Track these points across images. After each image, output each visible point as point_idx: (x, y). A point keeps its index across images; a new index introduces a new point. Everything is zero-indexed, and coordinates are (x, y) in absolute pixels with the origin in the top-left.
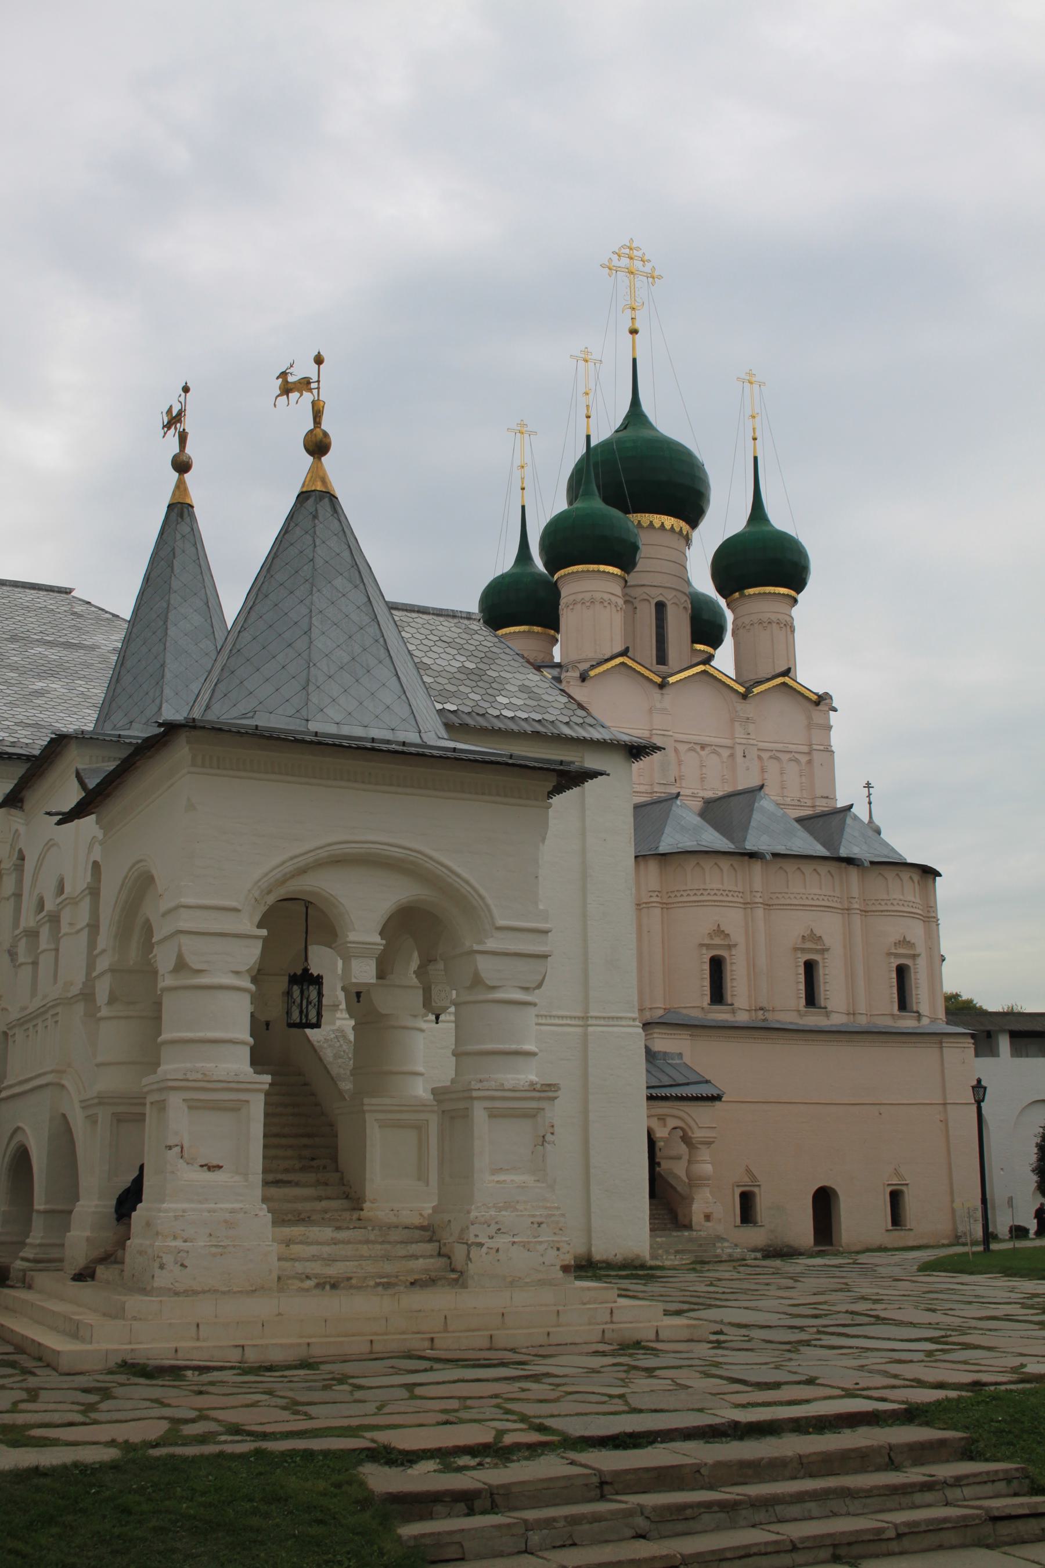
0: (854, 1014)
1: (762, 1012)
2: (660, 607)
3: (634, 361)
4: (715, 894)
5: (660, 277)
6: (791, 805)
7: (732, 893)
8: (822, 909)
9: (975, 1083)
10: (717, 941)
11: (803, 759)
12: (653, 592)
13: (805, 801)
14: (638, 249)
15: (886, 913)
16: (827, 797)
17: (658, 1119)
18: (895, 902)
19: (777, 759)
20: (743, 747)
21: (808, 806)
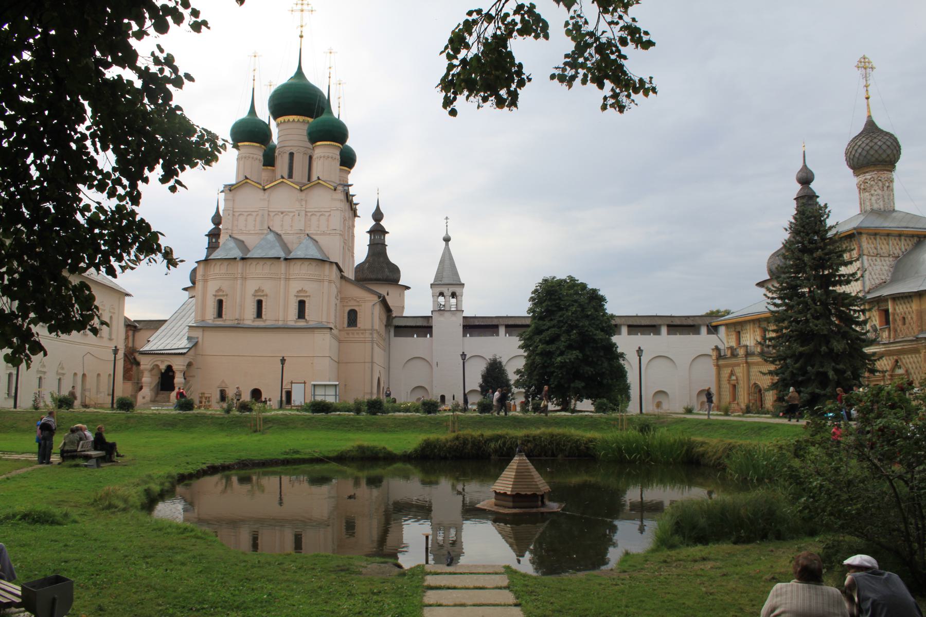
2: (292, 155)
10: (221, 293)
11: (327, 214)
12: (288, 149)
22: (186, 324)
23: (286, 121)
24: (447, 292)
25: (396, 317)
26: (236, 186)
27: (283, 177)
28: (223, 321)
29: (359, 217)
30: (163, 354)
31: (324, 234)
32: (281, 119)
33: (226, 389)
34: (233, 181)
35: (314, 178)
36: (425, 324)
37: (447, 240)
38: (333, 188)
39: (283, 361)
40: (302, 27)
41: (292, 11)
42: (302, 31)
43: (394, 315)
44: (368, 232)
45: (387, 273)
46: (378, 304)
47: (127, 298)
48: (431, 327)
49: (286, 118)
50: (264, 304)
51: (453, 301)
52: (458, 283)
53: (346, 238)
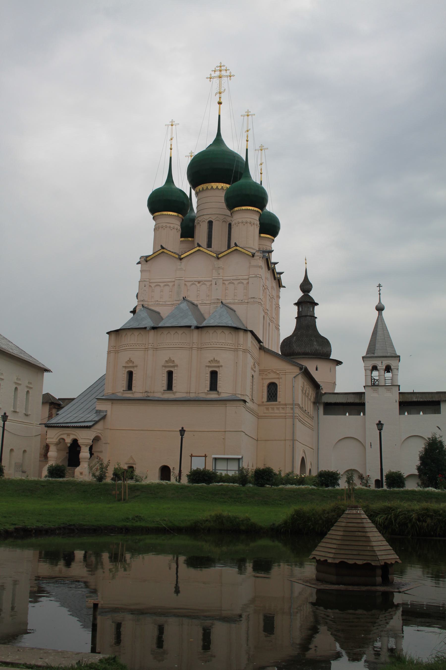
0: (189, 393)
1: (146, 393)
2: (210, 223)
3: (219, 116)
4: (179, 344)
5: (234, 76)
6: (237, 303)
7: (139, 345)
8: (179, 349)
9: (3, 414)
10: (131, 365)
13: (244, 300)
14: (224, 66)
15: (208, 349)
16: (254, 298)
17: (68, 435)
18: (212, 343)
19: (233, 283)
20: (216, 280)
21: (246, 303)
22: (94, 396)
23: (205, 189)
24: (381, 365)
25: (325, 393)
26: (153, 256)
27: (199, 245)
28: (133, 393)
29: (284, 287)
30: (68, 427)
31: (241, 303)
32: (200, 187)
33: (134, 466)
34: (149, 252)
35: (232, 244)
36: (357, 401)
37: (380, 309)
38: (250, 254)
39: (182, 432)
40: (220, 93)
41: (210, 78)
42: (220, 98)
43: (323, 392)
44: (295, 304)
45: (316, 346)
46: (300, 377)
47: (46, 374)
48: (364, 404)
49: (204, 186)
50: (174, 375)
51: (388, 375)
52: (393, 355)
53: (268, 307)
